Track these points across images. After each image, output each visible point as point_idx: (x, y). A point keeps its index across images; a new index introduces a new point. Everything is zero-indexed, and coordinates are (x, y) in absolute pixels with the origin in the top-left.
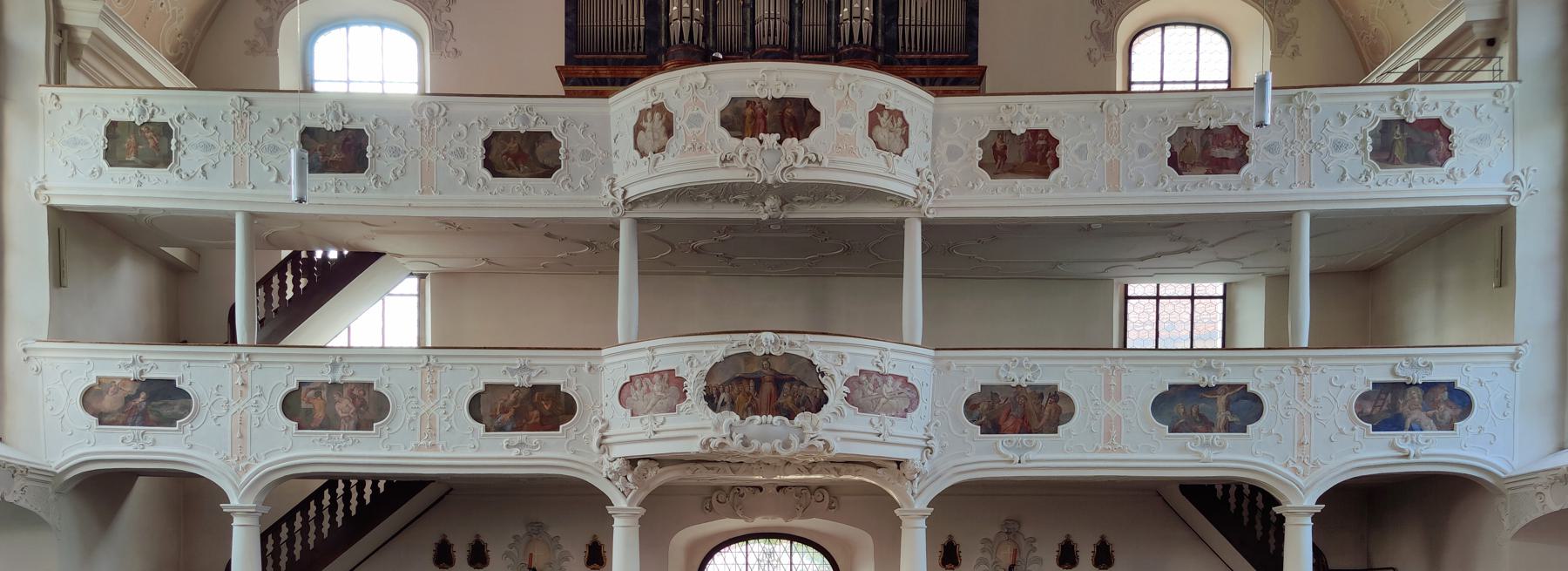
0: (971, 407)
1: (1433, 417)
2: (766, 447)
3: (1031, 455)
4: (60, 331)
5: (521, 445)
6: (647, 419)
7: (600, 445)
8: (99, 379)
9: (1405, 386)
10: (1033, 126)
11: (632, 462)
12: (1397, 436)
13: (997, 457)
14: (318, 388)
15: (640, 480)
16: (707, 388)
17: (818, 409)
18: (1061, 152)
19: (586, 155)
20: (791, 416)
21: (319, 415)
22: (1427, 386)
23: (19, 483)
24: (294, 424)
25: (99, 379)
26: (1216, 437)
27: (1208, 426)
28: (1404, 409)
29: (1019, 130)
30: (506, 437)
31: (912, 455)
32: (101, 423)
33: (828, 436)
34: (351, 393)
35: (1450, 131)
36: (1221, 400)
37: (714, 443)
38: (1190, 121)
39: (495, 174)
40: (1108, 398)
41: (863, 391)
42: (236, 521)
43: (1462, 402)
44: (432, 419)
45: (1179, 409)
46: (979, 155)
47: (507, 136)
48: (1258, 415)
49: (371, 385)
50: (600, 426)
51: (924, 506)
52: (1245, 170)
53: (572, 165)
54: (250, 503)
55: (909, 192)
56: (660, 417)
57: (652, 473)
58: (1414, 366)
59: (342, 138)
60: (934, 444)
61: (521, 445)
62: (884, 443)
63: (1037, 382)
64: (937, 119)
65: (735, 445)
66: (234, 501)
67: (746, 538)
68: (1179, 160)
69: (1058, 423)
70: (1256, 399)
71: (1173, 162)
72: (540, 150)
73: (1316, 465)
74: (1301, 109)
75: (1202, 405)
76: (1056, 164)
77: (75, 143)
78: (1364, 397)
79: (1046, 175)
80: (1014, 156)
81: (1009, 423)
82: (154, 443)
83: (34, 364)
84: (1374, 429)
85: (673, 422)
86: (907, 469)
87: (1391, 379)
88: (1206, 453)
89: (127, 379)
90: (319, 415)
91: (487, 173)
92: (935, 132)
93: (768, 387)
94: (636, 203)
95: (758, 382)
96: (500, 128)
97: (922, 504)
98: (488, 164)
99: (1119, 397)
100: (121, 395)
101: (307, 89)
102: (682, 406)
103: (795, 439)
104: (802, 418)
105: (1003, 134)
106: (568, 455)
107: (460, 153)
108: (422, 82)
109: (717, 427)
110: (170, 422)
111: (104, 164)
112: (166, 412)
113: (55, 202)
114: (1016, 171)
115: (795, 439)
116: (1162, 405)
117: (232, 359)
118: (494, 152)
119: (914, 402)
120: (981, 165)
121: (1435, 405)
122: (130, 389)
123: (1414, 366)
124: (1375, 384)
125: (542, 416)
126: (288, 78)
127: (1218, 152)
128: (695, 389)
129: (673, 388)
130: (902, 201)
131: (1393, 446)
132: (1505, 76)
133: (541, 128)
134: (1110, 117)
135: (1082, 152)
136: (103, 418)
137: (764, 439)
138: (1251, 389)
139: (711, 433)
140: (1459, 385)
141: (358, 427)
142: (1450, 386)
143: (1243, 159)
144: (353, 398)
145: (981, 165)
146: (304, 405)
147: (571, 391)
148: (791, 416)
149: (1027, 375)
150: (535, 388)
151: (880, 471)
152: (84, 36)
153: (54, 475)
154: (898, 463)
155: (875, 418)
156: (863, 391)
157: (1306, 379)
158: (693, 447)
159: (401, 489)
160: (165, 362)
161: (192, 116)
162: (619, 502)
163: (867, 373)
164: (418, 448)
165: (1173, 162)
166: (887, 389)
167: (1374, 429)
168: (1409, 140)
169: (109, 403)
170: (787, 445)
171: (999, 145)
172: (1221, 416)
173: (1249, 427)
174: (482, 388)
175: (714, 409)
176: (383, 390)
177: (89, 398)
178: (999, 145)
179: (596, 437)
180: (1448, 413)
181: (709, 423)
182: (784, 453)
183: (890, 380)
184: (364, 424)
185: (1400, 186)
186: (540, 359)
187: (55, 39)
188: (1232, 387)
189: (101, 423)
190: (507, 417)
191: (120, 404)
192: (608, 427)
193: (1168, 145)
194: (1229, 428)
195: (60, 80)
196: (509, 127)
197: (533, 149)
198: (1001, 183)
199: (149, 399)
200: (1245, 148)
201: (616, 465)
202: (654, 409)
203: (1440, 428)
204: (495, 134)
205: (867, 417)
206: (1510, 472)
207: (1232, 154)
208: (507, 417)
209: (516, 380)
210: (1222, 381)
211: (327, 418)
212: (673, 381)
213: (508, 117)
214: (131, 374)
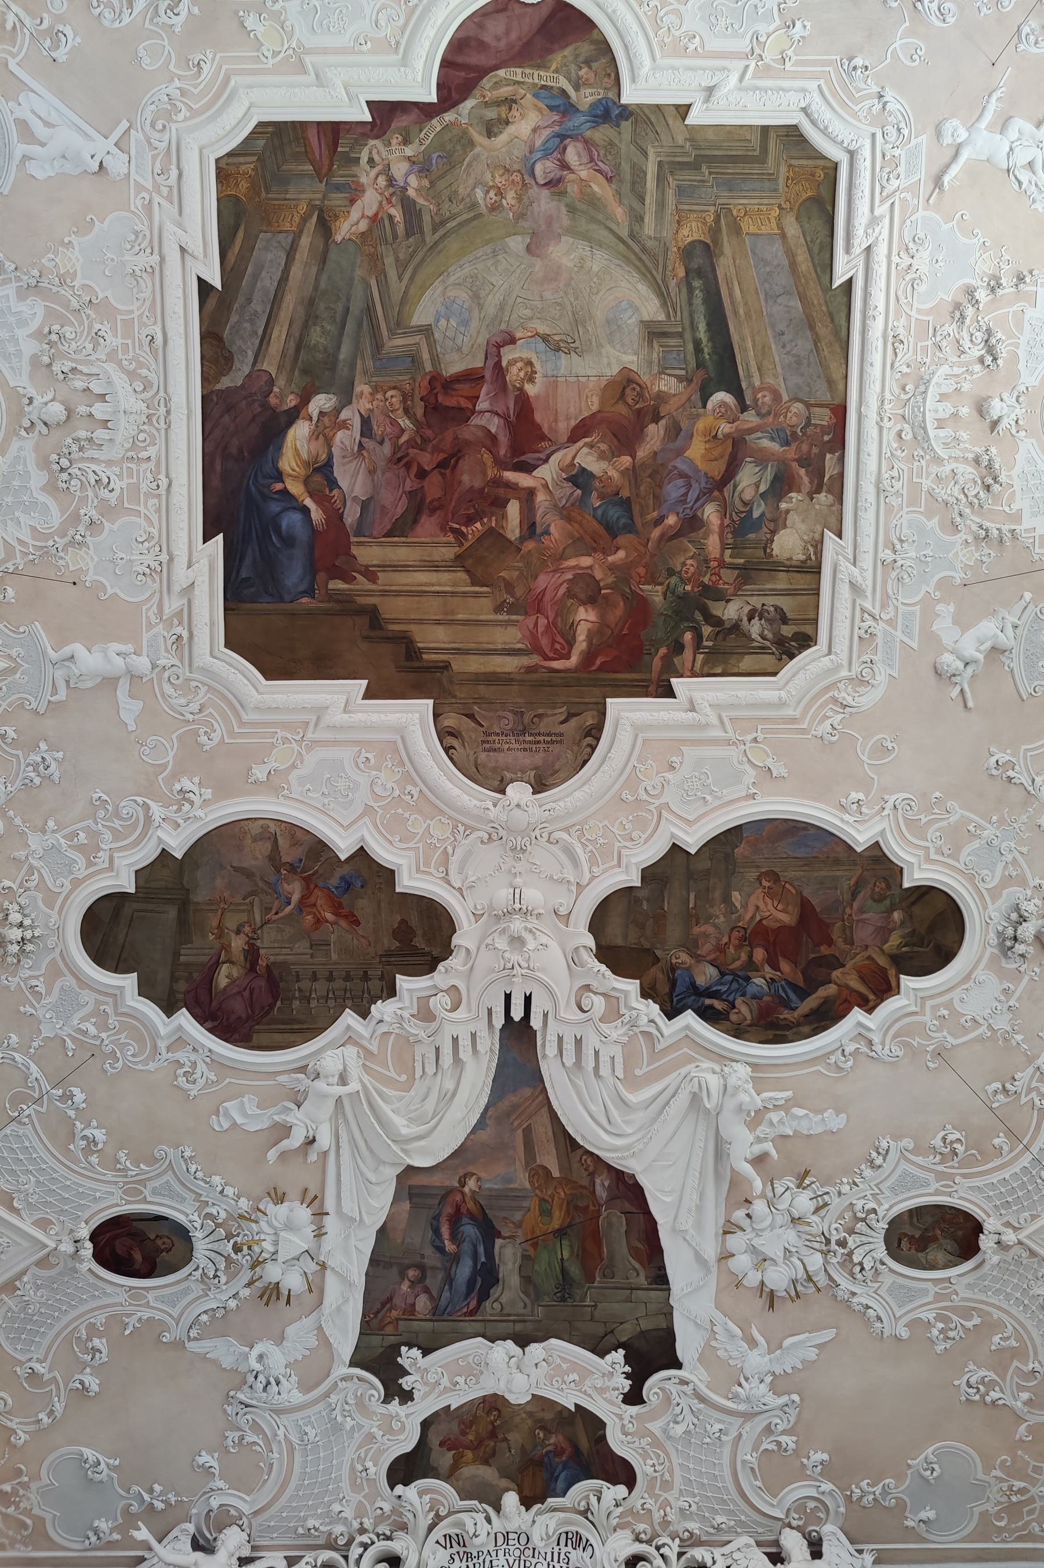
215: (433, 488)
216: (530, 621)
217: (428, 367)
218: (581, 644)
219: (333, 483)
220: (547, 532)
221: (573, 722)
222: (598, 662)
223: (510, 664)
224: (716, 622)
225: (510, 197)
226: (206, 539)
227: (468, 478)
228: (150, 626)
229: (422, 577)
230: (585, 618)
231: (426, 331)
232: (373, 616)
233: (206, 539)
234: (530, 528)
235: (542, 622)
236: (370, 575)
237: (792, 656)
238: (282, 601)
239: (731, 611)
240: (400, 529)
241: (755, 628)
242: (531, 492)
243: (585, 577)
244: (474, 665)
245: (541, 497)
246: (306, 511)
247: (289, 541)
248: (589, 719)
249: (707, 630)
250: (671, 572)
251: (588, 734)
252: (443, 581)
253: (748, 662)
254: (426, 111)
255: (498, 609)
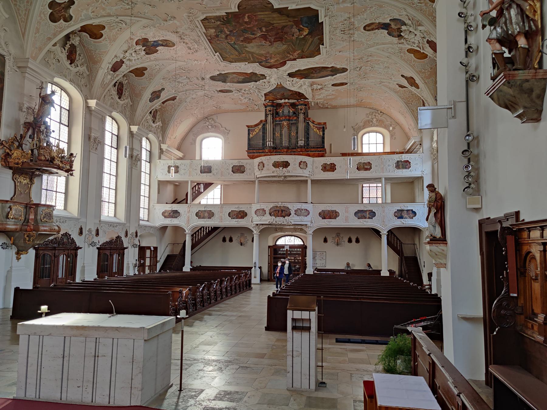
0: (320, 214)
1: (409, 216)
2: (280, 223)
3: (331, 223)
4: (158, 202)
5: (237, 221)
6: (259, 217)
7: (251, 221)
8: (165, 210)
9: (403, 210)
10: (331, 162)
11: (257, 225)
12: (402, 220)
13: (325, 224)
14: (202, 211)
15: (258, 228)
16: (270, 212)
17: (289, 216)
18: (336, 167)
19: (250, 169)
20: (284, 217)
21: (202, 216)
22: (408, 211)
23: (152, 229)
24: (198, 218)
25: (165, 210)
26: (367, 220)
27: (365, 218)
28: (403, 215)
29: (328, 163)
30: (235, 220)
31: (309, 224)
32: (165, 218)
33: (291, 221)
34: (207, 212)
35: (410, 163)
36: (368, 213)
37: (271, 222)
38: (360, 161)
39: (234, 173)
40: (346, 212)
41: (298, 212)
42: (187, 235)
43: (415, 213)
44: (222, 217)
45: (359, 215)
46: (321, 168)
47: (236, 166)
48: (375, 216)
49: (211, 211)
50: (252, 218)
51: (311, 233)
52: (371, 170)
53: (247, 171)
54: (189, 232)
55: (308, 175)
56: (262, 217)
57: (261, 226)
58: (405, 206)
59: (207, 167)
60: (313, 221)
61: (237, 221)
62: (302, 221)
63: (332, 209)
64: (313, 161)
65: (274, 222)
66: (187, 232)
67: (285, 236)
68: (359, 168)
69: (336, 217)
70: (374, 213)
71: (357, 169)
72: (242, 168)
73: (386, 226)
74: (382, 159)
75: (364, 214)
76: (336, 169)
77: (163, 169)
78: (395, 212)
79: (334, 171)
80: (328, 168)
81: (327, 217)
82: (174, 221)
83: (154, 208)
84: (398, 218)
85: (264, 218)
86: (307, 226)
87: (401, 209)
88: (364, 223)
89: (169, 210)
90: (202, 216)
91: (232, 173)
92: (313, 164)
93: (280, 212)
94: (258, 178)
95: (279, 211)
96: (235, 165)
97: (311, 232)
98: (232, 171)
99: (348, 213)
100: (169, 213)
101: (201, 159)
102: (265, 215)
103: (285, 221)
104: (286, 218)
105: (325, 164)
106: (246, 223)
107: (228, 169)
108: (222, 158)
109: (271, 219)
110: (176, 218)
111: (167, 173)
112: (176, 216)
113: (159, 180)
114: (328, 171)
115: (285, 221)
116: (356, 214)
117: (187, 206)
118: (234, 169)
119: (309, 214)
120: (322, 170)
121: (409, 214)
122: (170, 212)
123: (405, 206)
124: (397, 210)
125: (241, 216)
126: (197, 157)
127: (366, 167)
128: (267, 212)
129: (264, 212)
130: (307, 177)
131: (401, 222)
132: (421, 152)
133: (243, 165)
134: (345, 161)
135: (340, 167)
136: (165, 217)
137: (279, 222)
138: (373, 211)
139: (270, 220)
140: (413, 210)
141: (209, 218)
142: (412, 210)
143: (371, 168)
144: (208, 213)
145: (322, 170)
146: (199, 214)
147: (246, 211)
148: (284, 217)
149: (331, 208)
150: (240, 211)
151: (303, 226)
152: (164, 150)
153: (157, 227)
154: (306, 225)
155: (300, 217)
156: (298, 212)
157: (384, 209)
158: (267, 223)
159: (215, 229)
160: (175, 207)
161: (182, 164)
162: (255, 232)
163: (299, 209)
164: (219, 222)
165: (357, 169)
166: (303, 212)
167: (398, 218)
168: (402, 164)
169: (166, 214)
170: (283, 222)
171: (325, 166)
172: (368, 216)
173: (373, 218)
174: (230, 211)
175: (271, 216)
176: (213, 211)
177: (163, 214)
178: (325, 166)
179: (251, 220)
180: (412, 216)
181: (270, 218)
182: (283, 224)
183: (304, 210)
184: (210, 218)
185: (401, 173)
186: (241, 206)
187: (160, 151)
188: (370, 210)
189: (165, 218)
190: (235, 216)
191: (168, 215)
192: (253, 218)
193: (356, 166)
194: (369, 218)
195: (160, 158)
196: (236, 165)
197: (240, 168)
198: (326, 173)
199: (173, 213)
200: (371, 166)
201: (254, 225)
202: (260, 215)
203: (410, 218)
204: (234, 166)
205: (299, 217)
206: (424, 227)
207: (369, 167)
208: (235, 216)
209: (237, 210)
210: (368, 209)
211: (203, 217)
212: (264, 210)
213: (236, 163)
214: (170, 209)
215: (280, 31)
216: (257, 18)
217: (283, 42)
218: (246, 18)
219: (298, 30)
220: (257, 29)
221: (244, 7)
222: (242, 15)
223: (259, 13)
224: (221, 21)
225: (273, 56)
226: (323, 22)
227: (274, 33)
228: (334, 10)
229: (280, 22)
230: (246, 19)
231: (284, 45)
232: (288, 16)
233: (323, 22)
234: (261, 29)
235: (255, 19)
236: (290, 21)
237: (205, 18)
238: (307, 16)
239: (219, 23)
240: (285, 27)
241: (213, 21)
242: (261, 32)
243: (248, 25)
244: (267, 13)
245: (260, 32)
246: (303, 26)
247: (306, 23)
248: (241, 8)
249: (222, 20)
250: (232, 26)
251: (240, 6)
252: (275, 22)
253: (213, 17)
254: (287, 61)
255: (263, 20)
